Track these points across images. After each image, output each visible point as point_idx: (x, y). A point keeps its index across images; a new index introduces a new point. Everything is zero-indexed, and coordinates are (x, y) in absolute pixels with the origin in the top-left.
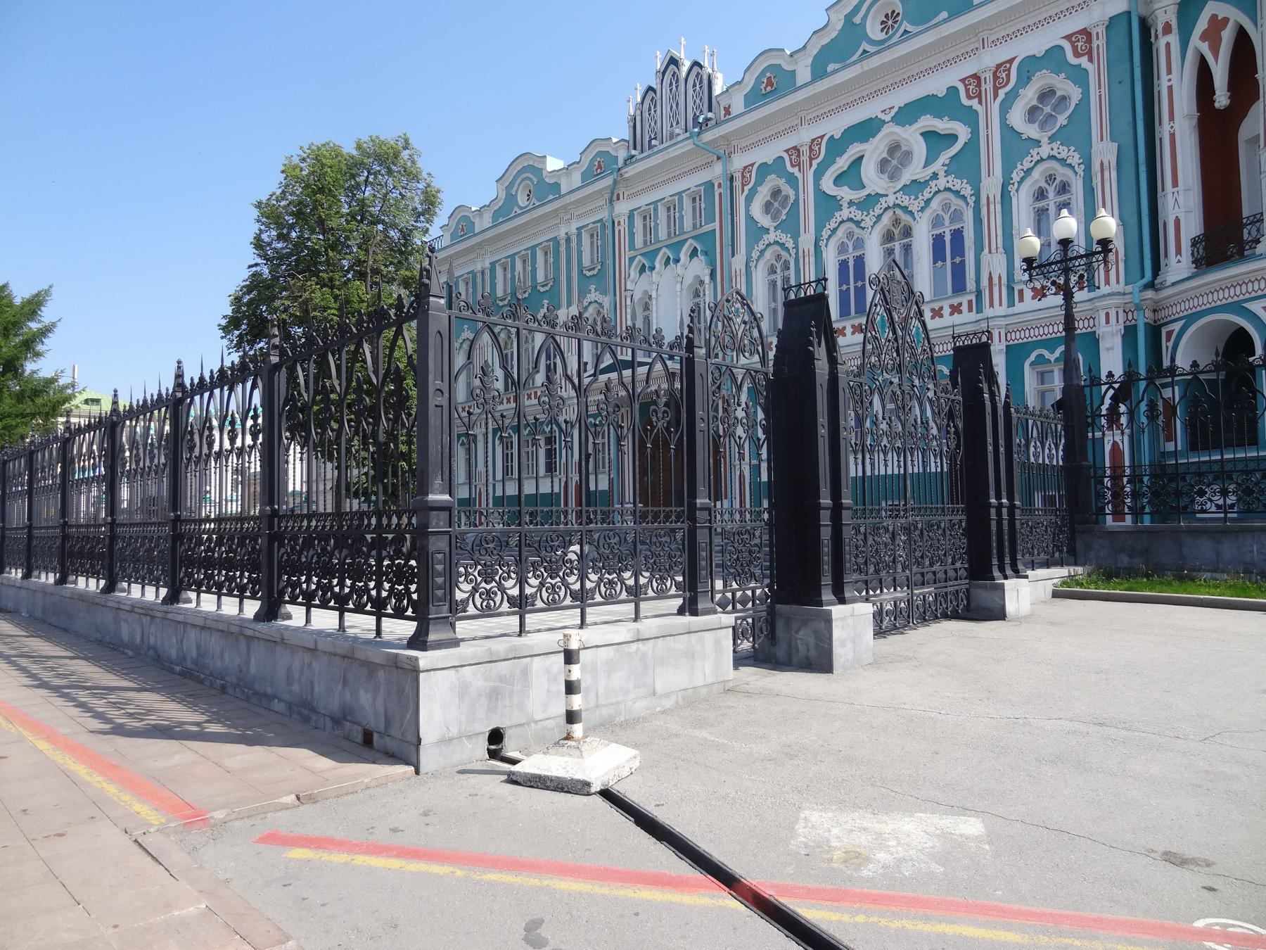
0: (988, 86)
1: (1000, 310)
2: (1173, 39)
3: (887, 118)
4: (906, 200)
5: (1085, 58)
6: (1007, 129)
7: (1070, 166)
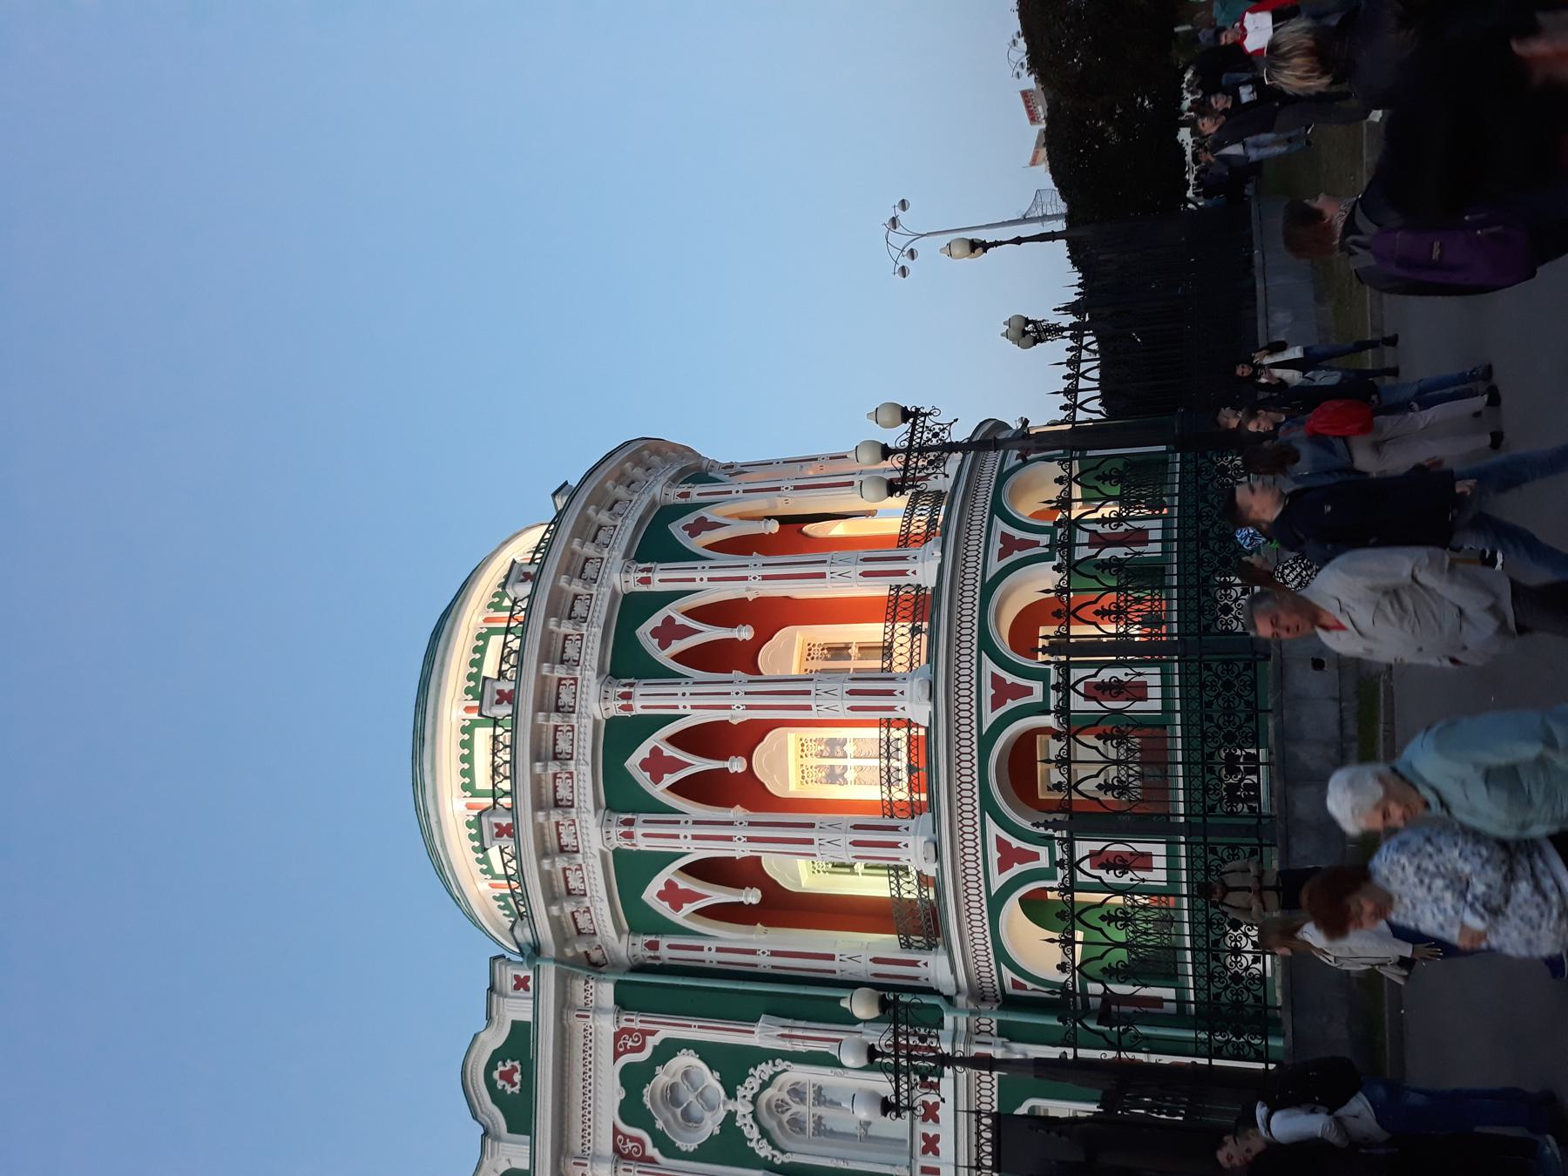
2: (664, 942)
5: (649, 1038)
7: (772, 1078)
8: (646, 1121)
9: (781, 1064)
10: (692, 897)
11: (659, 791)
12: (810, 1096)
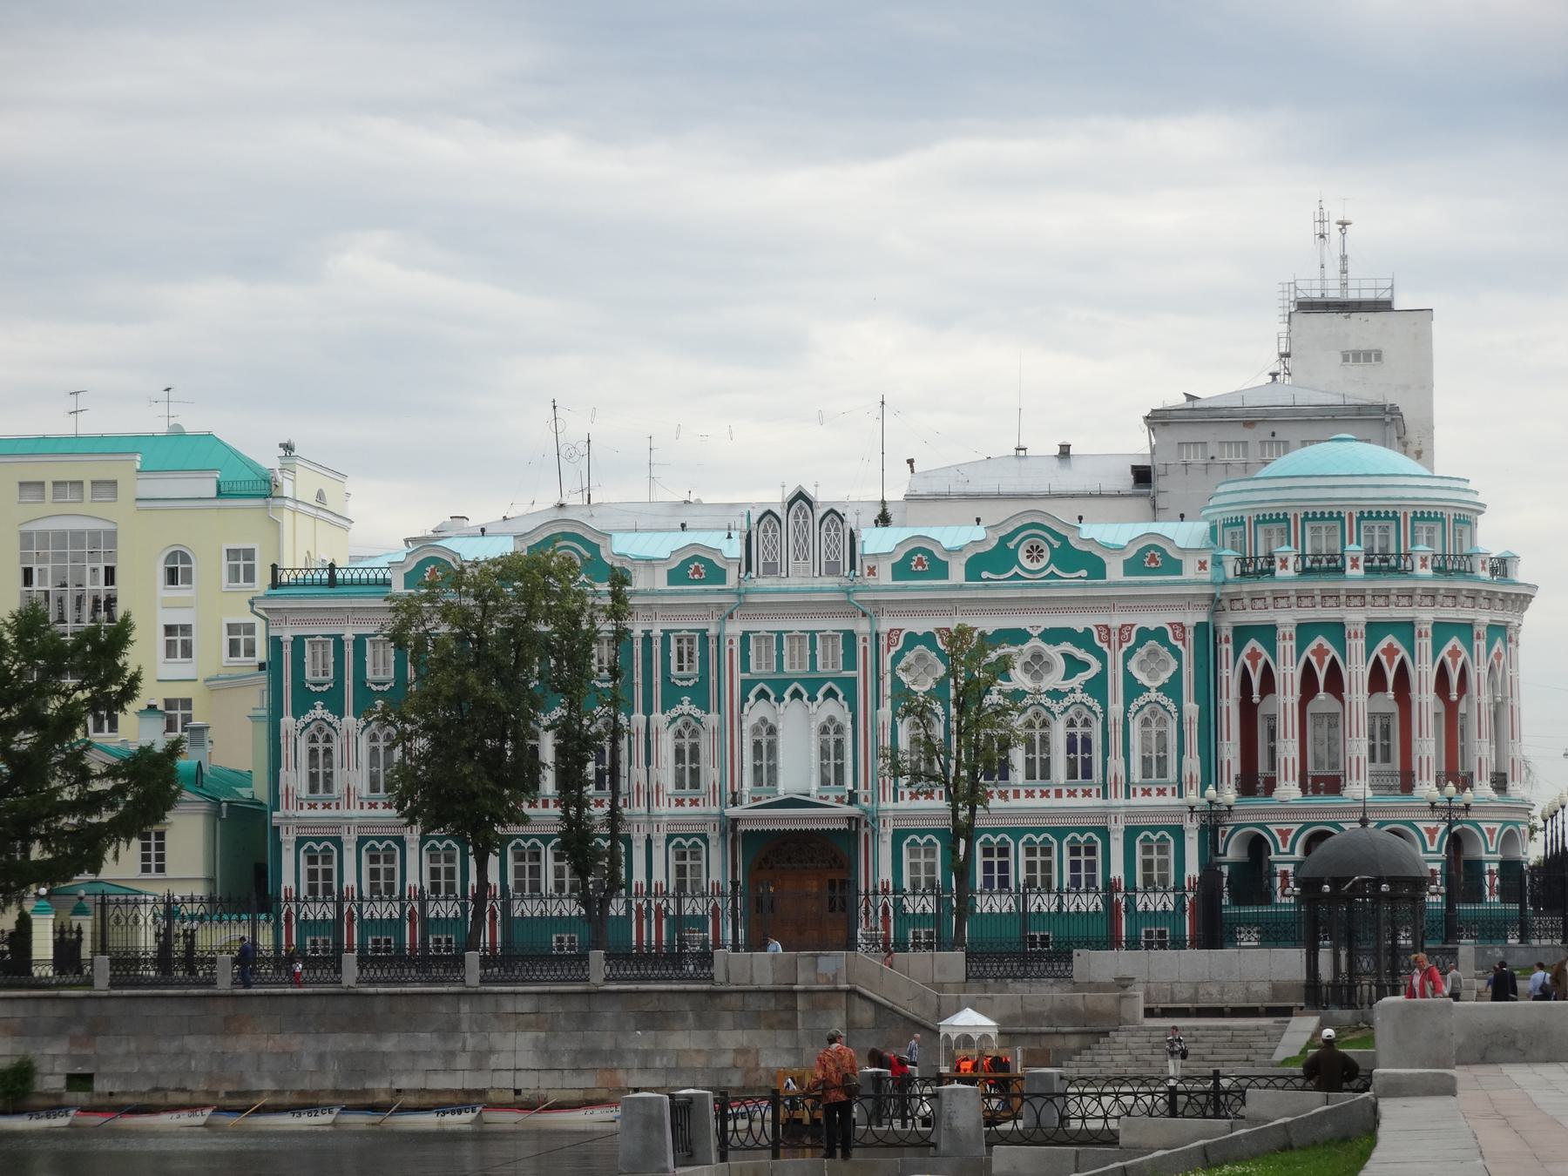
0: (1115, 638)
1: (1121, 801)
2: (1230, 647)
3: (1035, 634)
4: (1048, 702)
6: (1128, 675)
9: (1176, 716)
10: (1255, 666)
11: (1307, 653)
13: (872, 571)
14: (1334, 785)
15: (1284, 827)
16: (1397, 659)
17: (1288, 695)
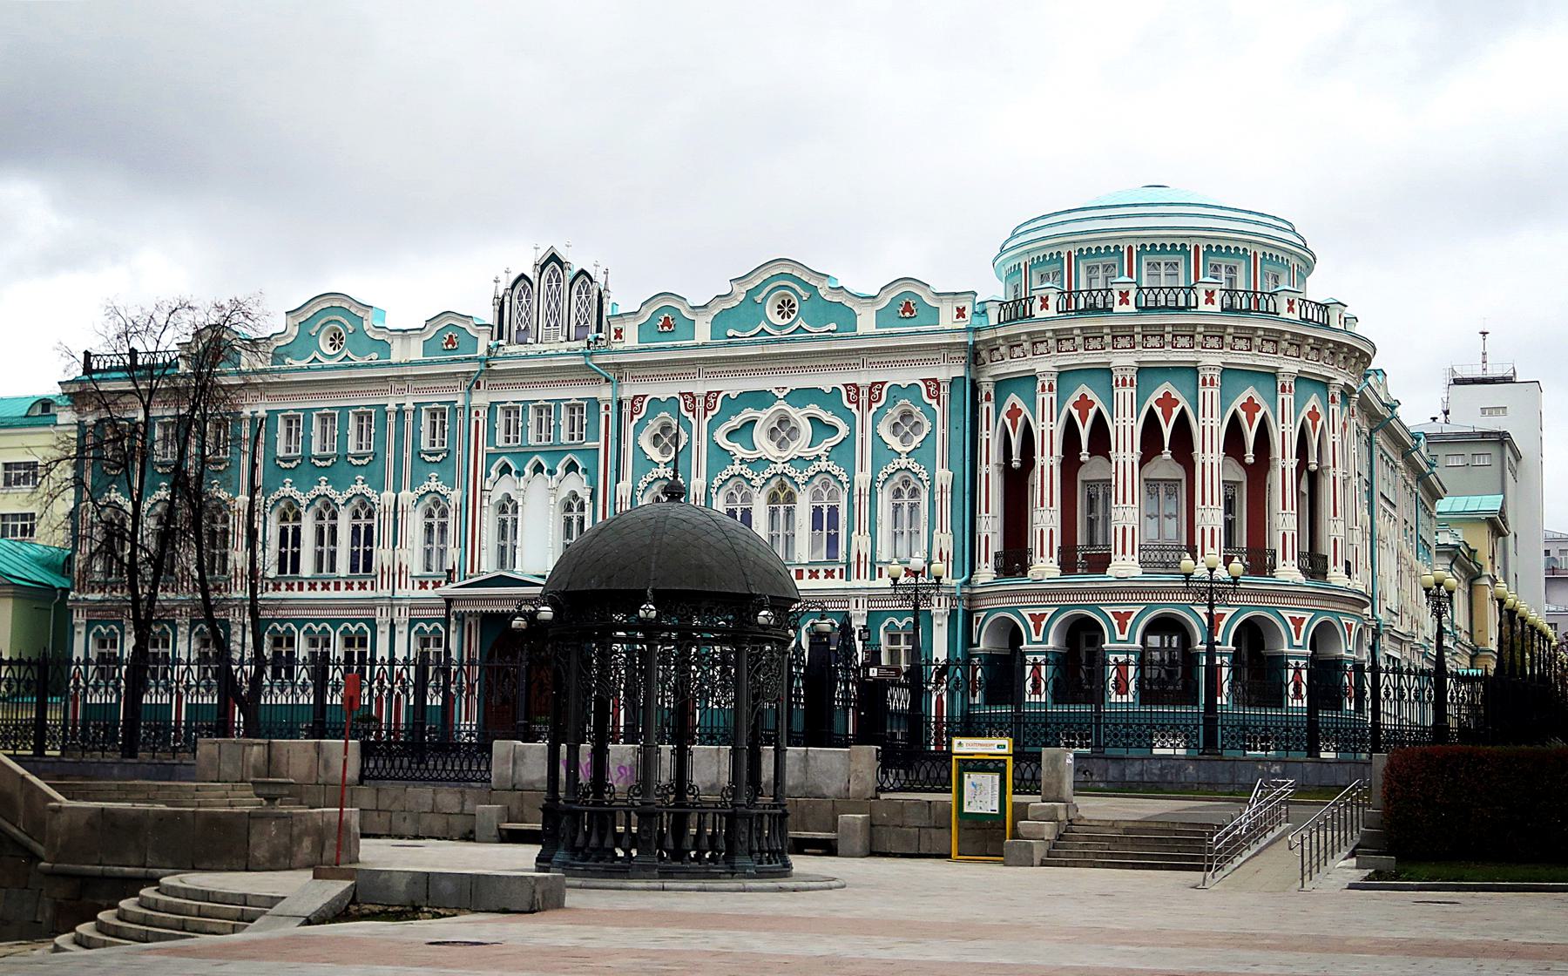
1: (864, 582)
2: (992, 406)
8: (891, 401)
11: (1069, 405)
12: (913, 501)
13: (619, 333)
14: (1100, 563)
15: (1037, 612)
16: (1176, 411)
17: (1048, 460)
